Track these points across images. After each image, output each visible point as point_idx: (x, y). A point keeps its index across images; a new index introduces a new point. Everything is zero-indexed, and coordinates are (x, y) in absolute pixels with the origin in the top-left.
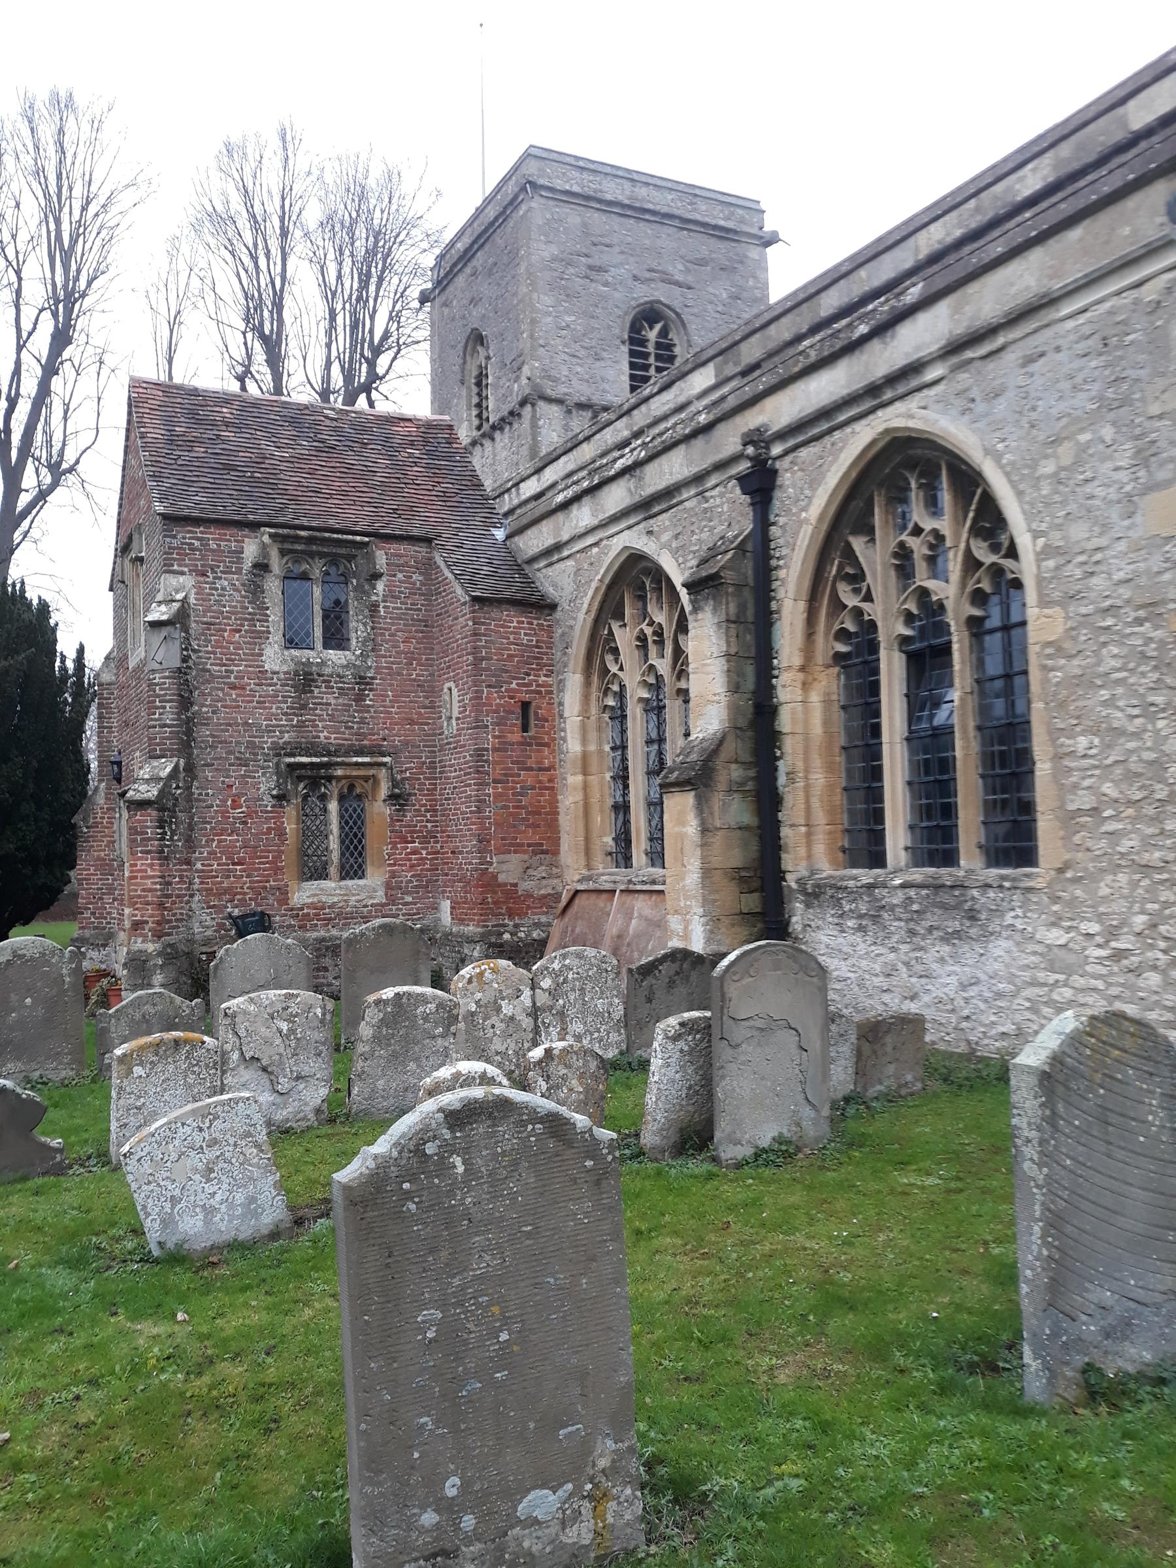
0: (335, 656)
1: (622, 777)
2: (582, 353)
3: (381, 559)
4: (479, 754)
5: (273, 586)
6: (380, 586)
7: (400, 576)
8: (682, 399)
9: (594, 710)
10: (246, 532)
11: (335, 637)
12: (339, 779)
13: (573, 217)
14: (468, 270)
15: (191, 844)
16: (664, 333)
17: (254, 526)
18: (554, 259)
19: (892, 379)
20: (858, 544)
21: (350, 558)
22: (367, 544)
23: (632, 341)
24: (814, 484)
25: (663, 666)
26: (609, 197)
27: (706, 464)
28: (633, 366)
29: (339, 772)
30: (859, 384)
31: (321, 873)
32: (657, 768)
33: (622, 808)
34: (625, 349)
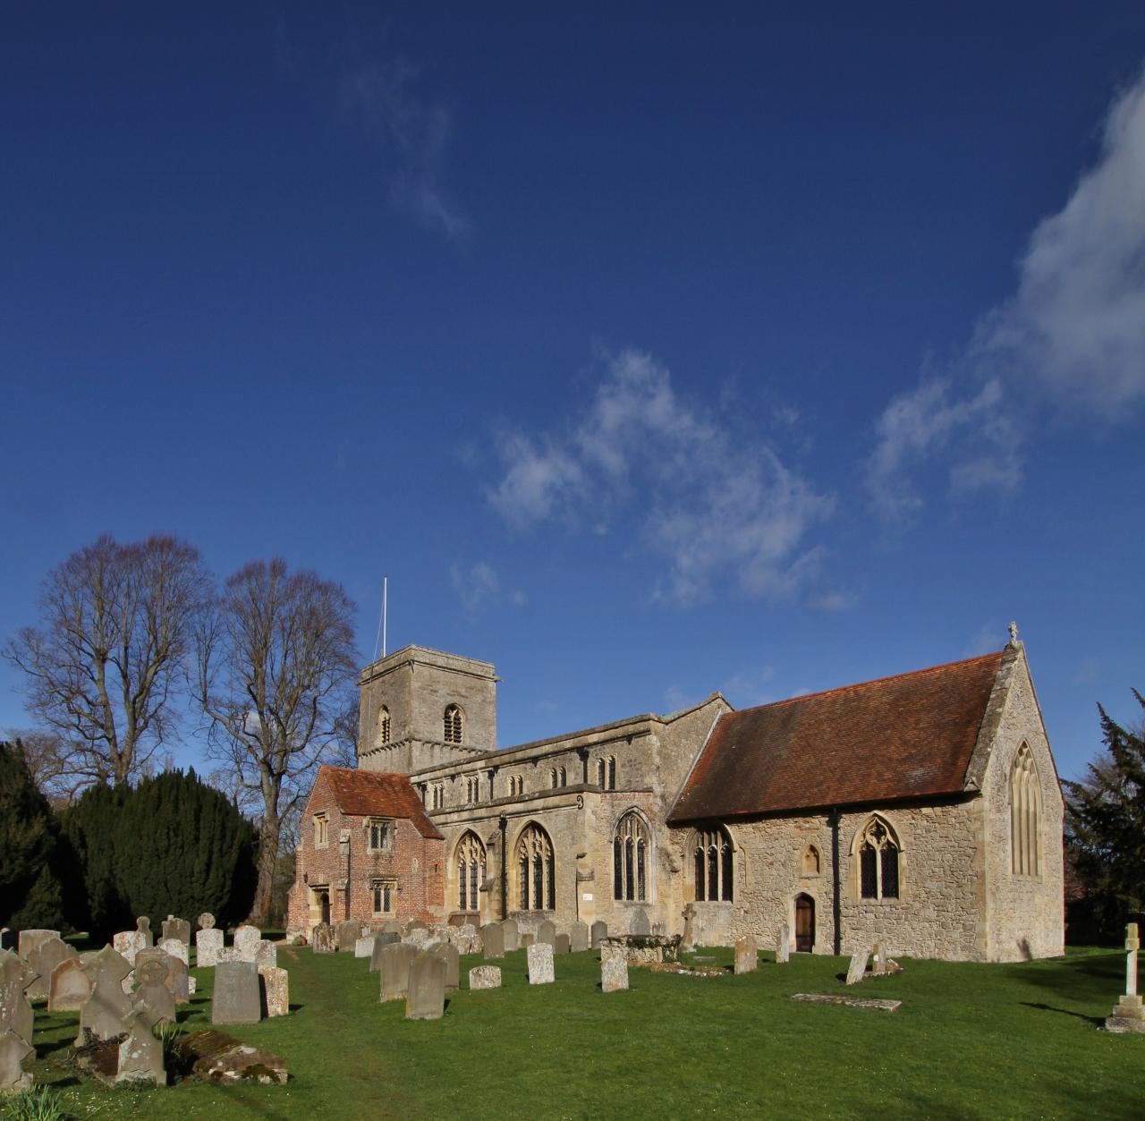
1: (463, 886)
2: (428, 722)
3: (397, 823)
4: (424, 878)
5: (369, 831)
8: (474, 767)
9: (455, 867)
13: (426, 671)
14: (381, 680)
16: (457, 713)
18: (419, 687)
19: (532, 811)
20: (525, 840)
23: (446, 717)
24: (516, 825)
25: (478, 859)
26: (439, 664)
27: (490, 815)
28: (446, 726)
30: (526, 810)
32: (474, 885)
33: (463, 894)
34: (443, 721)
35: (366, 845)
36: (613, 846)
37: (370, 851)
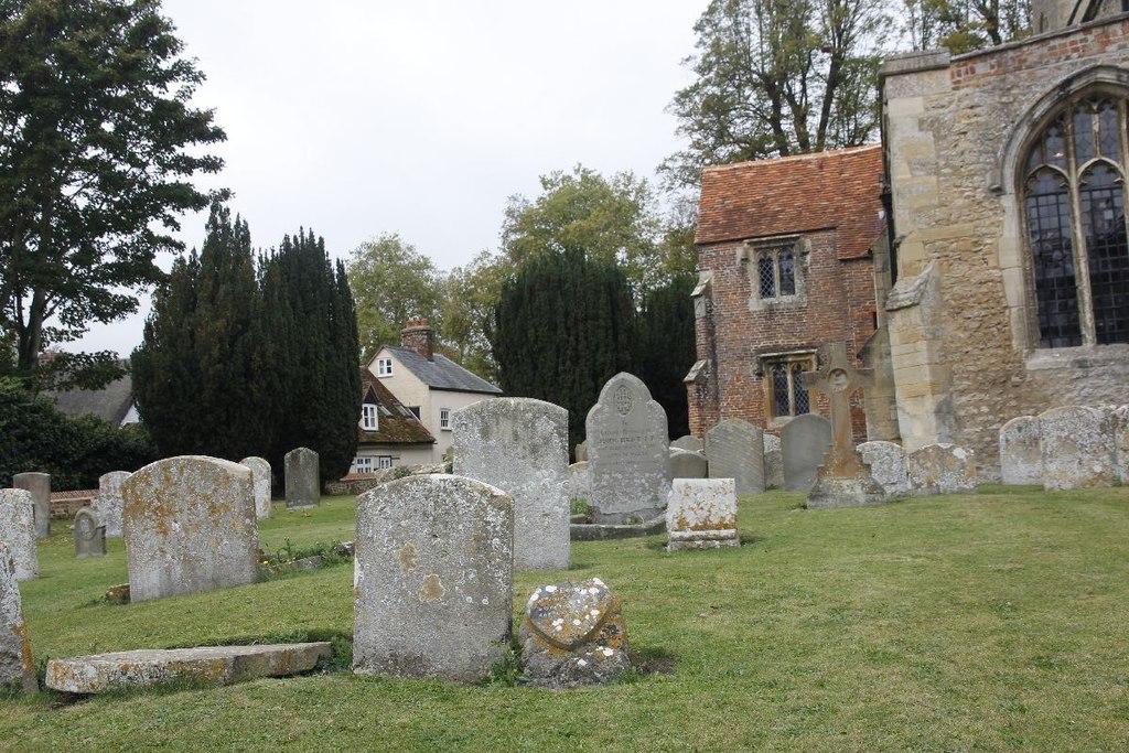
0: (787, 299)
3: (808, 243)
5: (753, 270)
6: (808, 258)
7: (820, 251)
10: (737, 243)
11: (788, 287)
12: (791, 363)
15: (717, 399)
17: (741, 240)
21: (792, 246)
22: (798, 238)
29: (790, 359)
31: (785, 412)
35: (746, 294)
36: (1009, 202)
37: (755, 304)
